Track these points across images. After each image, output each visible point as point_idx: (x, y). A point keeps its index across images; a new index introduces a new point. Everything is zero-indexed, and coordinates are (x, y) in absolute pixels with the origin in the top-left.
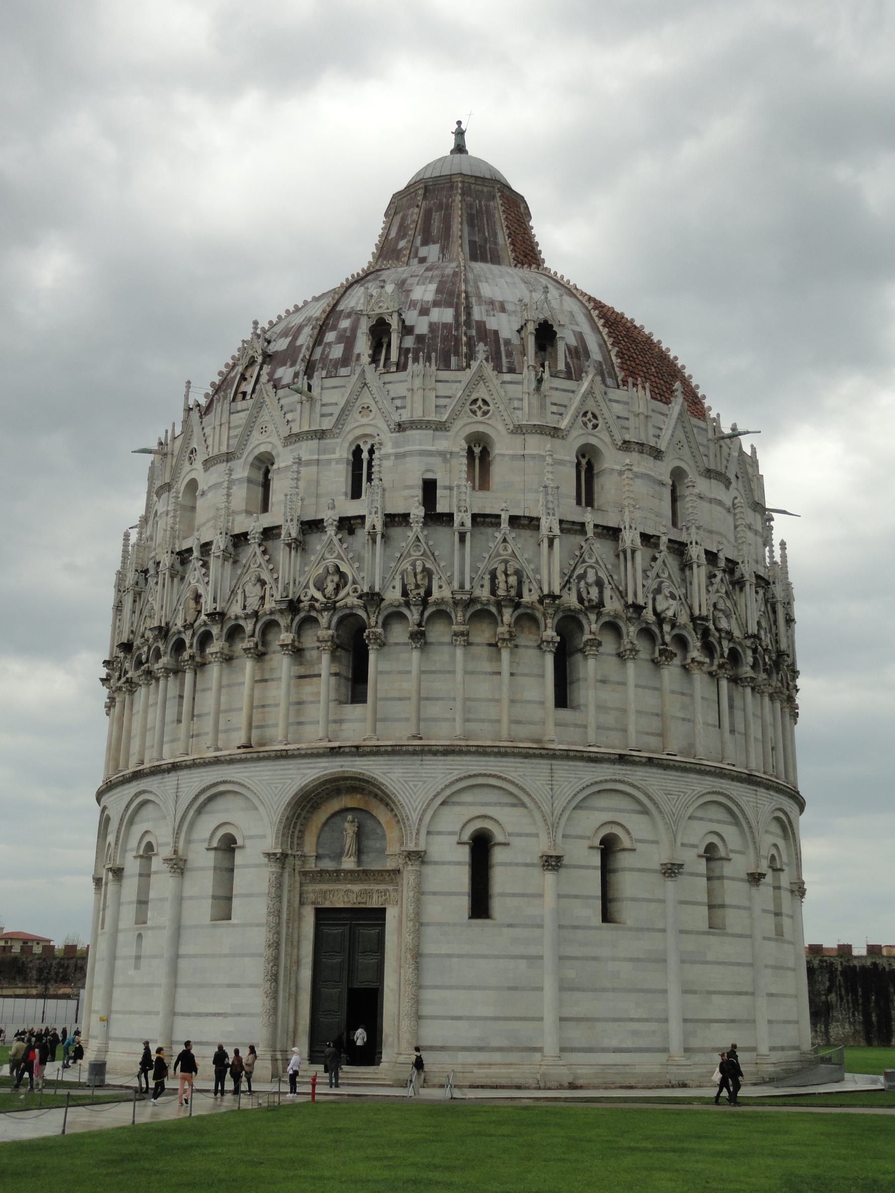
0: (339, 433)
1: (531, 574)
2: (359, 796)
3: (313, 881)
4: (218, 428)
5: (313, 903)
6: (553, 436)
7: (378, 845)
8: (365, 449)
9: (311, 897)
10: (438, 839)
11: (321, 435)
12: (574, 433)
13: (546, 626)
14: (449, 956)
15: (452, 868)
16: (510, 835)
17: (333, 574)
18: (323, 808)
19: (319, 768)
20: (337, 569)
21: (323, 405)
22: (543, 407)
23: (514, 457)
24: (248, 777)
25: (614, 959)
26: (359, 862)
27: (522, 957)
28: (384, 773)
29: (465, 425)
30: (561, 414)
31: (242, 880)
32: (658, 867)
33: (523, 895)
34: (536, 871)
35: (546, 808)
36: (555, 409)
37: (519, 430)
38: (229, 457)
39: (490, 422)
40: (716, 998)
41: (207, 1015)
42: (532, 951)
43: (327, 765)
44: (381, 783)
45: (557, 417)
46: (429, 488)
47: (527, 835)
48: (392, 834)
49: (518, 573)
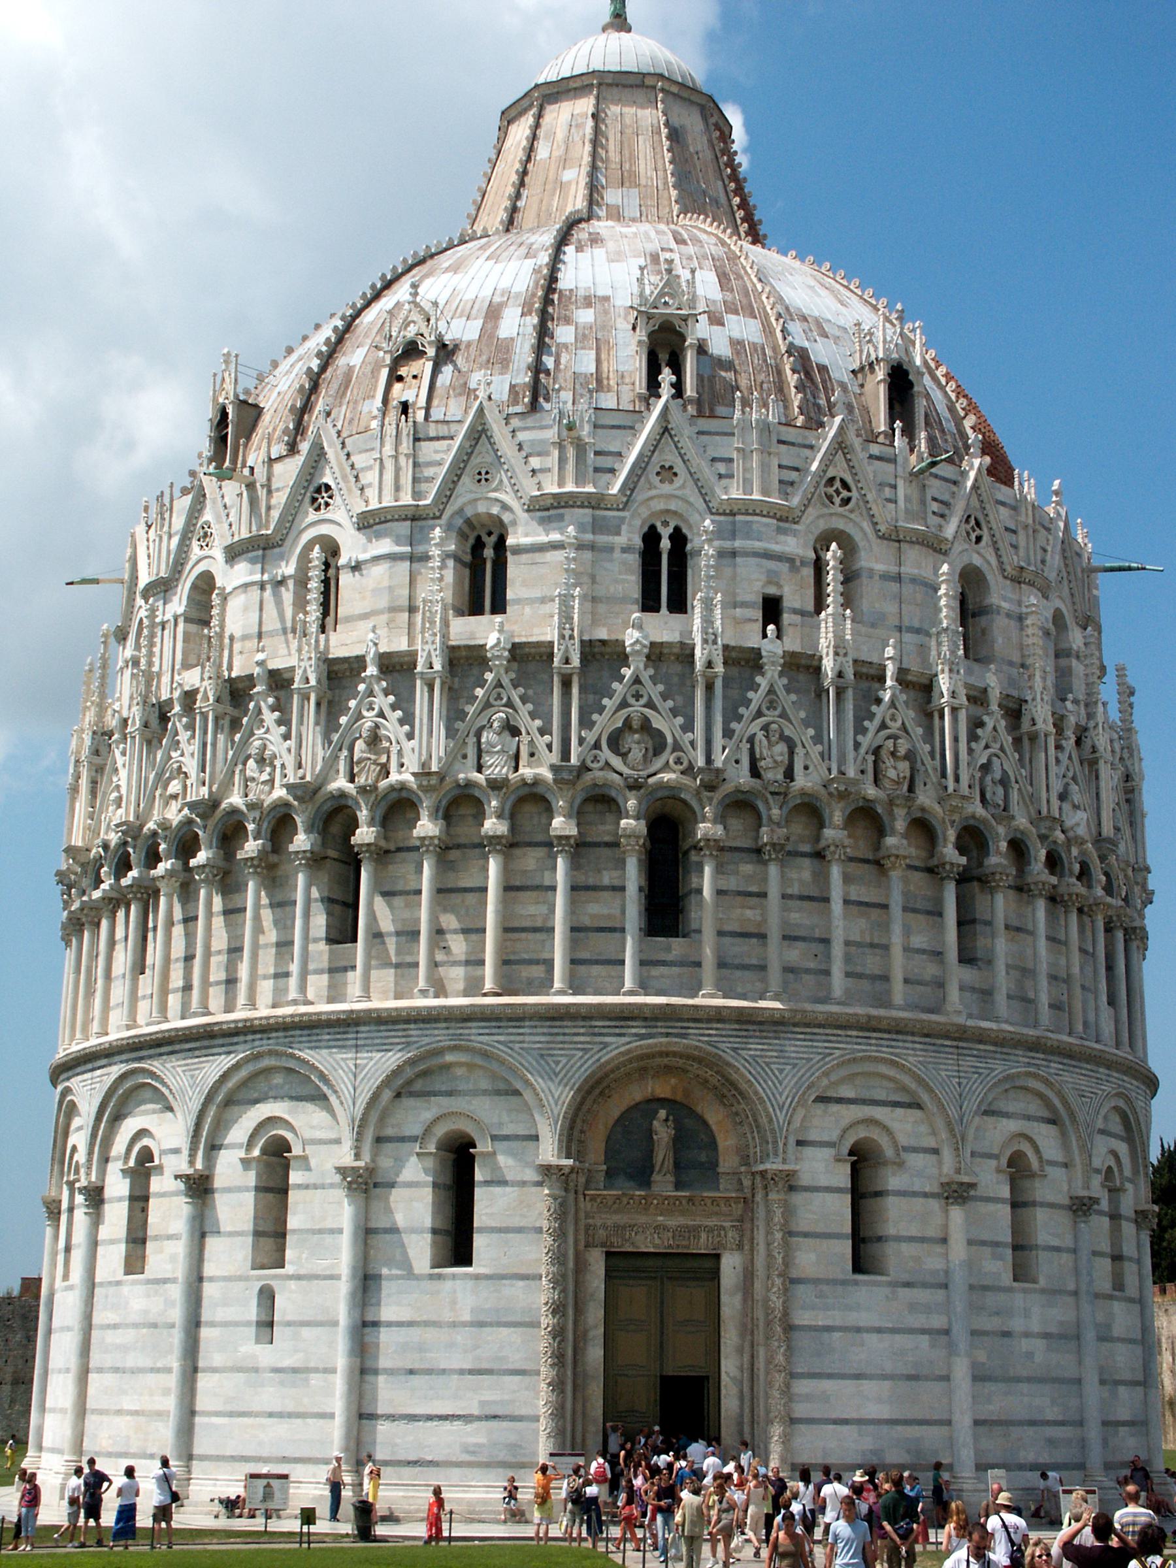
0: (626, 503)
1: (927, 760)
2: (673, 1081)
4: (389, 465)
5: (603, 1245)
6: (935, 550)
7: (703, 1158)
8: (665, 533)
10: (808, 1151)
11: (595, 502)
12: (958, 547)
13: (945, 840)
14: (829, 1329)
15: (829, 1197)
16: (905, 1149)
17: (636, 732)
20: (646, 722)
21: (597, 453)
22: (923, 502)
23: (885, 577)
25: (1027, 1335)
26: (678, 1186)
27: (923, 1331)
28: (734, 1049)
29: (818, 517)
30: (942, 516)
31: (488, 1205)
32: (1067, 1202)
33: (922, 1240)
34: (935, 1205)
35: (953, 1112)
36: (935, 506)
37: (895, 538)
38: (416, 517)
39: (852, 516)
40: (1122, 1389)
41: (430, 1418)
42: (938, 1322)
43: (643, 1031)
44: (728, 1064)
45: (938, 520)
46: (772, 609)
47: (926, 1150)
48: (726, 1142)
49: (910, 756)
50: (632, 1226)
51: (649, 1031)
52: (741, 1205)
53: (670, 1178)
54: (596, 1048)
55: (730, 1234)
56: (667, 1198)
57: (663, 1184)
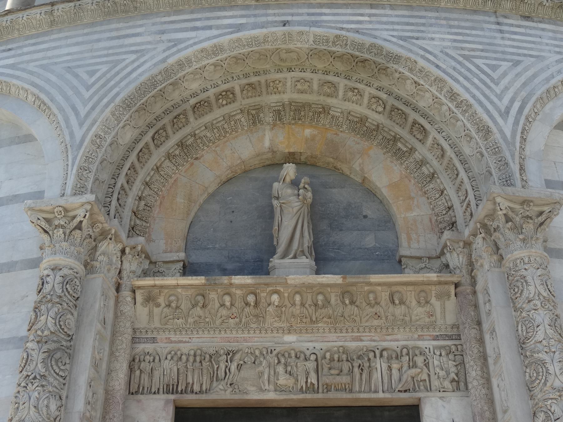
2: (308, 132)
5: (170, 389)
7: (370, 241)
19: (218, 27)
24: (12, 66)
43: (243, 21)
44: (397, 58)
50: (230, 354)
51: (252, 20)
52: (451, 303)
53: (307, 261)
54: (161, 47)
56: (299, 290)
57: (294, 272)
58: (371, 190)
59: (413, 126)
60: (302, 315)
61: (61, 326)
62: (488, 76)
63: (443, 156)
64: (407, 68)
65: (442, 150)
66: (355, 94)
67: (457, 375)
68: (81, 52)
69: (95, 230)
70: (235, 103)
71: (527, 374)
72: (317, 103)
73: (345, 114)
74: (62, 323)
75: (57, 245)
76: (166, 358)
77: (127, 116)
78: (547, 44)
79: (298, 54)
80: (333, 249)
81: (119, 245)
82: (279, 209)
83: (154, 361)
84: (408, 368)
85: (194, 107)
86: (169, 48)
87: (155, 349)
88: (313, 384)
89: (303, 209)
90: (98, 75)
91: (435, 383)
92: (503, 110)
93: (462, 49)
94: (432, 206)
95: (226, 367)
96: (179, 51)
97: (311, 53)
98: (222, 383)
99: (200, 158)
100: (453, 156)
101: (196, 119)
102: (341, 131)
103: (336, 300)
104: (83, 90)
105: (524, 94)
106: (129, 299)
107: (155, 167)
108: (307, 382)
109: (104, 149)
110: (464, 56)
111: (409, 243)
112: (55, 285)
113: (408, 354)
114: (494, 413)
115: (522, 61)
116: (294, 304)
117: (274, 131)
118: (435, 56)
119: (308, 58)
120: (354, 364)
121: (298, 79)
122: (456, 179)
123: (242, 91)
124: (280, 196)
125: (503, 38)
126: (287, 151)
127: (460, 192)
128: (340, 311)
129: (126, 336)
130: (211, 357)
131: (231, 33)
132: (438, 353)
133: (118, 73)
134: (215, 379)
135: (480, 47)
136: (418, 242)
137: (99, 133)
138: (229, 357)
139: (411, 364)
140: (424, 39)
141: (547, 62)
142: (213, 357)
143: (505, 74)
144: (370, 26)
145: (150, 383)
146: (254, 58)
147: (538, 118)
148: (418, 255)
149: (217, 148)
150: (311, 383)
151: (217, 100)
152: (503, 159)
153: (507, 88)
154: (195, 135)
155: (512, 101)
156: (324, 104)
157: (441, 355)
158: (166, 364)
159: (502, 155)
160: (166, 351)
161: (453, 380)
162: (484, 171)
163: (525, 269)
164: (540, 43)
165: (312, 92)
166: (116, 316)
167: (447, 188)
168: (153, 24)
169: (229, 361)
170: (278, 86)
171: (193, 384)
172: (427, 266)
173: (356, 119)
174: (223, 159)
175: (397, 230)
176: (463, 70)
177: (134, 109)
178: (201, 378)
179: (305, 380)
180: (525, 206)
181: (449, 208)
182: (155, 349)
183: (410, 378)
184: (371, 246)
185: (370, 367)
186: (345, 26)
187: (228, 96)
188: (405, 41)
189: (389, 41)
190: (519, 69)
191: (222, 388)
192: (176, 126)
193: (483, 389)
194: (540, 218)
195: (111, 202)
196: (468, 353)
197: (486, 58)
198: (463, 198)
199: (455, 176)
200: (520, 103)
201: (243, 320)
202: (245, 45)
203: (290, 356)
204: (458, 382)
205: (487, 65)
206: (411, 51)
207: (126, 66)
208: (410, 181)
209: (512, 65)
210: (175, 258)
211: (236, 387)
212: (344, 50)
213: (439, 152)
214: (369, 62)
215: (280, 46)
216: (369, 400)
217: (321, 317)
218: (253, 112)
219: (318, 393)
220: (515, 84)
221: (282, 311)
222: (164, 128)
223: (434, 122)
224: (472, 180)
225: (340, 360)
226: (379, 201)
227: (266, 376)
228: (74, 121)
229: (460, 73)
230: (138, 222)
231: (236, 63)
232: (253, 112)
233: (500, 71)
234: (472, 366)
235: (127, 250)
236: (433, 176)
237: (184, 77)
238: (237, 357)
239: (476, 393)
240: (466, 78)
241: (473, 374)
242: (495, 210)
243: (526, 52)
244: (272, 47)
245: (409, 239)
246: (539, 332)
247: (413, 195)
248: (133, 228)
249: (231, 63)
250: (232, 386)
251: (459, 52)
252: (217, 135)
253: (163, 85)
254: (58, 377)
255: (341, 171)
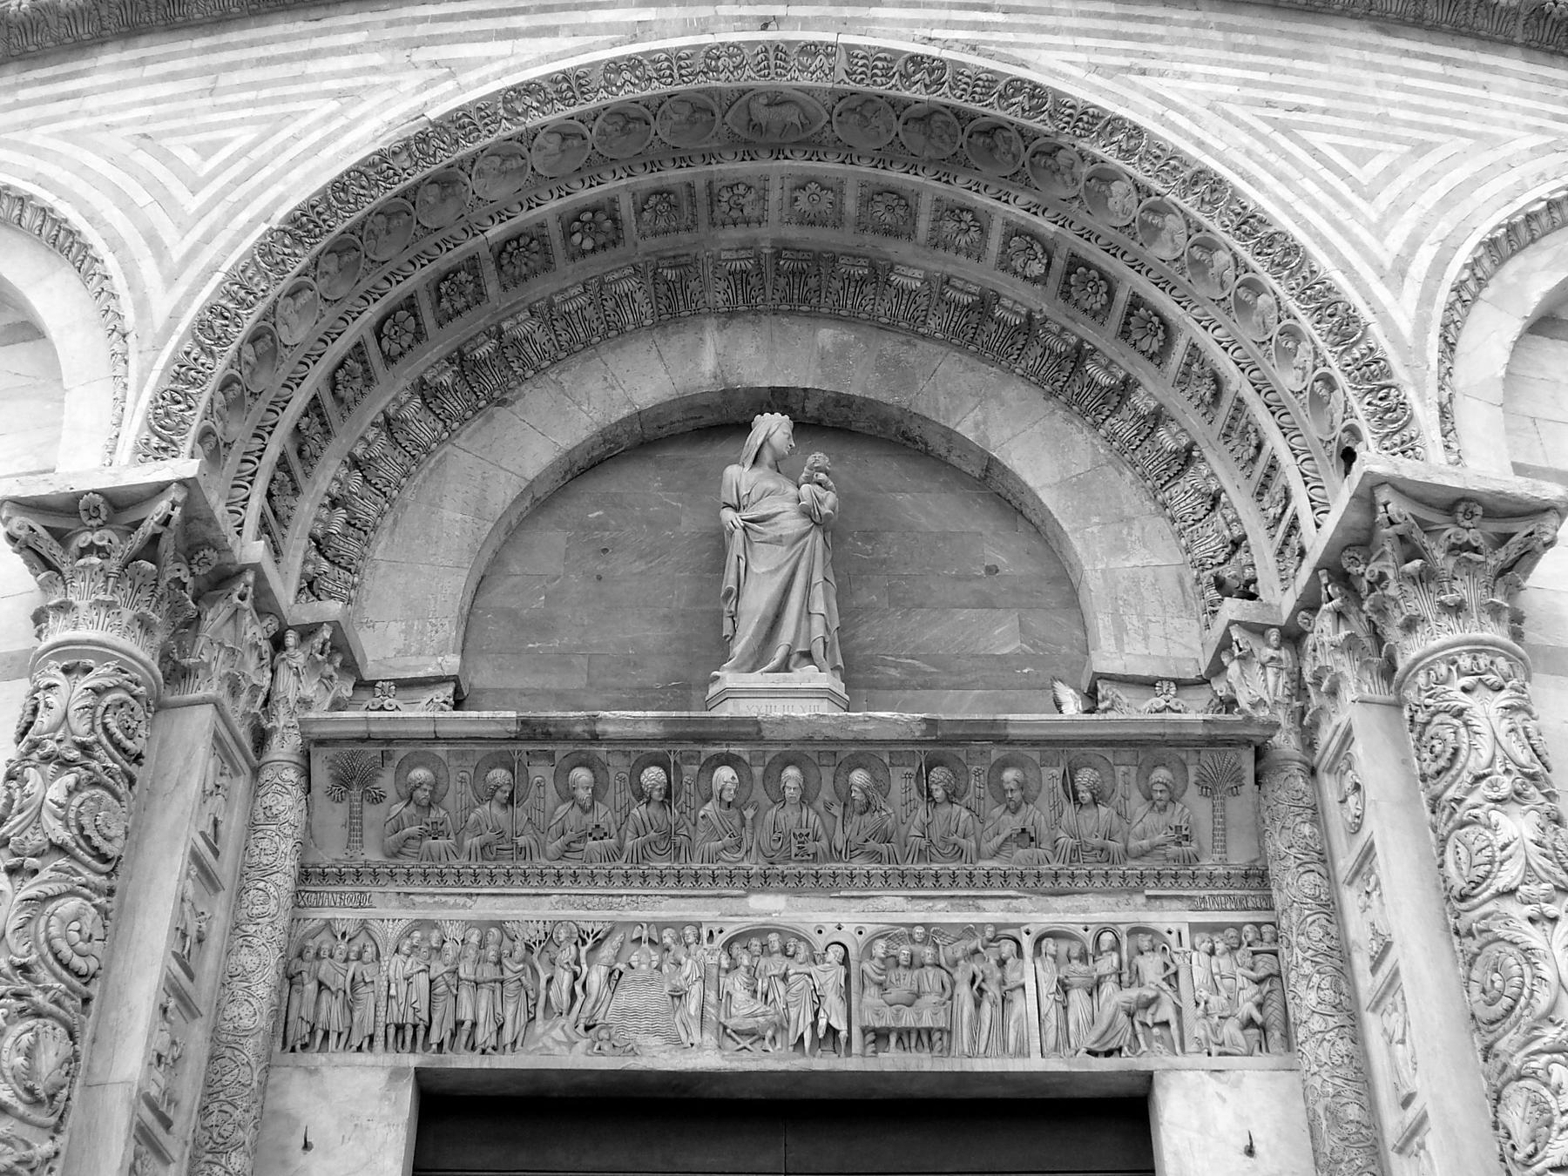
2: (827, 335)
3: (411, 858)
5: (403, 1035)
9: (400, 980)
18: (536, 399)
19: (575, 31)
55: (1198, 969)
58: (1009, 497)
59: (1130, 314)
60: (804, 832)
61: (82, 828)
62: (1344, 176)
63: (1217, 395)
64: (1114, 147)
65: (1217, 379)
66: (963, 226)
67: (1260, 1006)
68: (182, 97)
69: (196, 569)
70: (620, 247)
71: (1475, 989)
72: (855, 252)
73: (936, 288)
74: (85, 820)
75: (82, 604)
76: (397, 951)
77: (305, 261)
78: (1504, 107)
79: (802, 109)
80: (899, 656)
81: (268, 621)
82: (739, 533)
83: (359, 957)
84: (1116, 987)
85: (501, 250)
86: (430, 84)
87: (364, 925)
88: (836, 1032)
89: (810, 538)
90: (225, 153)
91: (1197, 1029)
92: (1388, 265)
93: (1269, 104)
94: (1183, 542)
95: (576, 977)
96: (461, 89)
97: (839, 107)
98: (562, 1021)
99: (513, 403)
100: (1248, 392)
101: (505, 288)
102: (923, 335)
103: (907, 790)
104: (179, 191)
105: (1444, 226)
106: (291, 775)
107: (381, 419)
108: (815, 1025)
109: (233, 347)
110: (1273, 122)
111: (1119, 641)
112: (71, 713)
113: (1116, 947)
114: (1370, 1106)
115: (1438, 144)
116: (780, 799)
117: (729, 332)
118: (1193, 118)
119: (830, 122)
120: (957, 976)
121: (800, 183)
122: (1253, 460)
123: (640, 211)
124: (744, 502)
125: (1379, 84)
126: (765, 384)
127: (1266, 498)
128: (917, 822)
129: (279, 878)
130: (529, 948)
131: (613, 45)
132: (1206, 946)
133: (283, 148)
134: (540, 1014)
135: (1319, 102)
136: (1146, 638)
137: (223, 302)
138: (583, 950)
139: (1125, 978)
140: (1161, 74)
141: (1505, 152)
142: (537, 949)
143: (1391, 173)
144: (1010, 37)
145: (348, 1021)
146: (675, 117)
147: (1487, 293)
148: (1145, 671)
149: (564, 375)
150: (829, 1026)
151: (568, 234)
152: (1393, 392)
153: (1397, 208)
154: (500, 332)
155: (1414, 243)
156: (873, 255)
157: (1212, 953)
158: (396, 966)
159: (1389, 382)
160: (393, 931)
161: (1250, 1023)
162: (1338, 431)
163: (1464, 690)
164: (1485, 103)
165: (838, 223)
166: (252, 826)
167: (1227, 486)
168: (390, 24)
169: (583, 960)
170: (742, 201)
171: (474, 1024)
172: (1171, 704)
173: (967, 299)
174: (579, 404)
175: (1083, 606)
176: (1272, 158)
177: (324, 242)
178: (499, 1009)
179: (810, 1018)
180: (1460, 517)
181: (1236, 544)
182: (364, 925)
183: (1122, 1017)
184: (1006, 651)
185: (1003, 982)
186: (935, 33)
187: (598, 224)
188: (1110, 77)
189: (1067, 76)
190: (1428, 162)
191: (561, 1037)
192: (445, 304)
193: (1339, 1042)
194: (1502, 554)
195: (247, 499)
196: (1293, 940)
197: (1339, 130)
198: (1275, 511)
199: (1252, 451)
200: (1435, 249)
201: (629, 843)
202: (650, 79)
203: (765, 949)
204: (1263, 1028)
205: (1342, 149)
206: (1125, 102)
207: (308, 130)
208: (1121, 474)
209: (1412, 152)
210: (431, 671)
211: (603, 1034)
212: (933, 97)
213: (1206, 390)
214: (1006, 134)
215: (751, 83)
216: (1002, 1077)
217: (860, 840)
218: (670, 274)
219: (849, 1054)
220: (1421, 201)
221: (743, 819)
222: (410, 304)
223: (1190, 301)
224: (1300, 459)
225: (916, 961)
226: (1032, 529)
227: (693, 1006)
228: (149, 270)
229: (1264, 165)
230: (325, 566)
231: (624, 131)
232: (670, 274)
233: (1377, 165)
234: (1308, 977)
235: (291, 638)
236: (1187, 457)
237: (473, 162)
238: (607, 951)
239: (1320, 1051)
240: (1281, 178)
241: (1311, 998)
242: (1372, 528)
243: (1446, 121)
244: (727, 85)
245: (1120, 630)
246: (1507, 865)
247: (1128, 510)
248: (310, 585)
249: (609, 129)
250: (591, 1032)
251: (1259, 111)
252: (564, 338)
253: (412, 180)
254: (65, 974)
255: (921, 446)
